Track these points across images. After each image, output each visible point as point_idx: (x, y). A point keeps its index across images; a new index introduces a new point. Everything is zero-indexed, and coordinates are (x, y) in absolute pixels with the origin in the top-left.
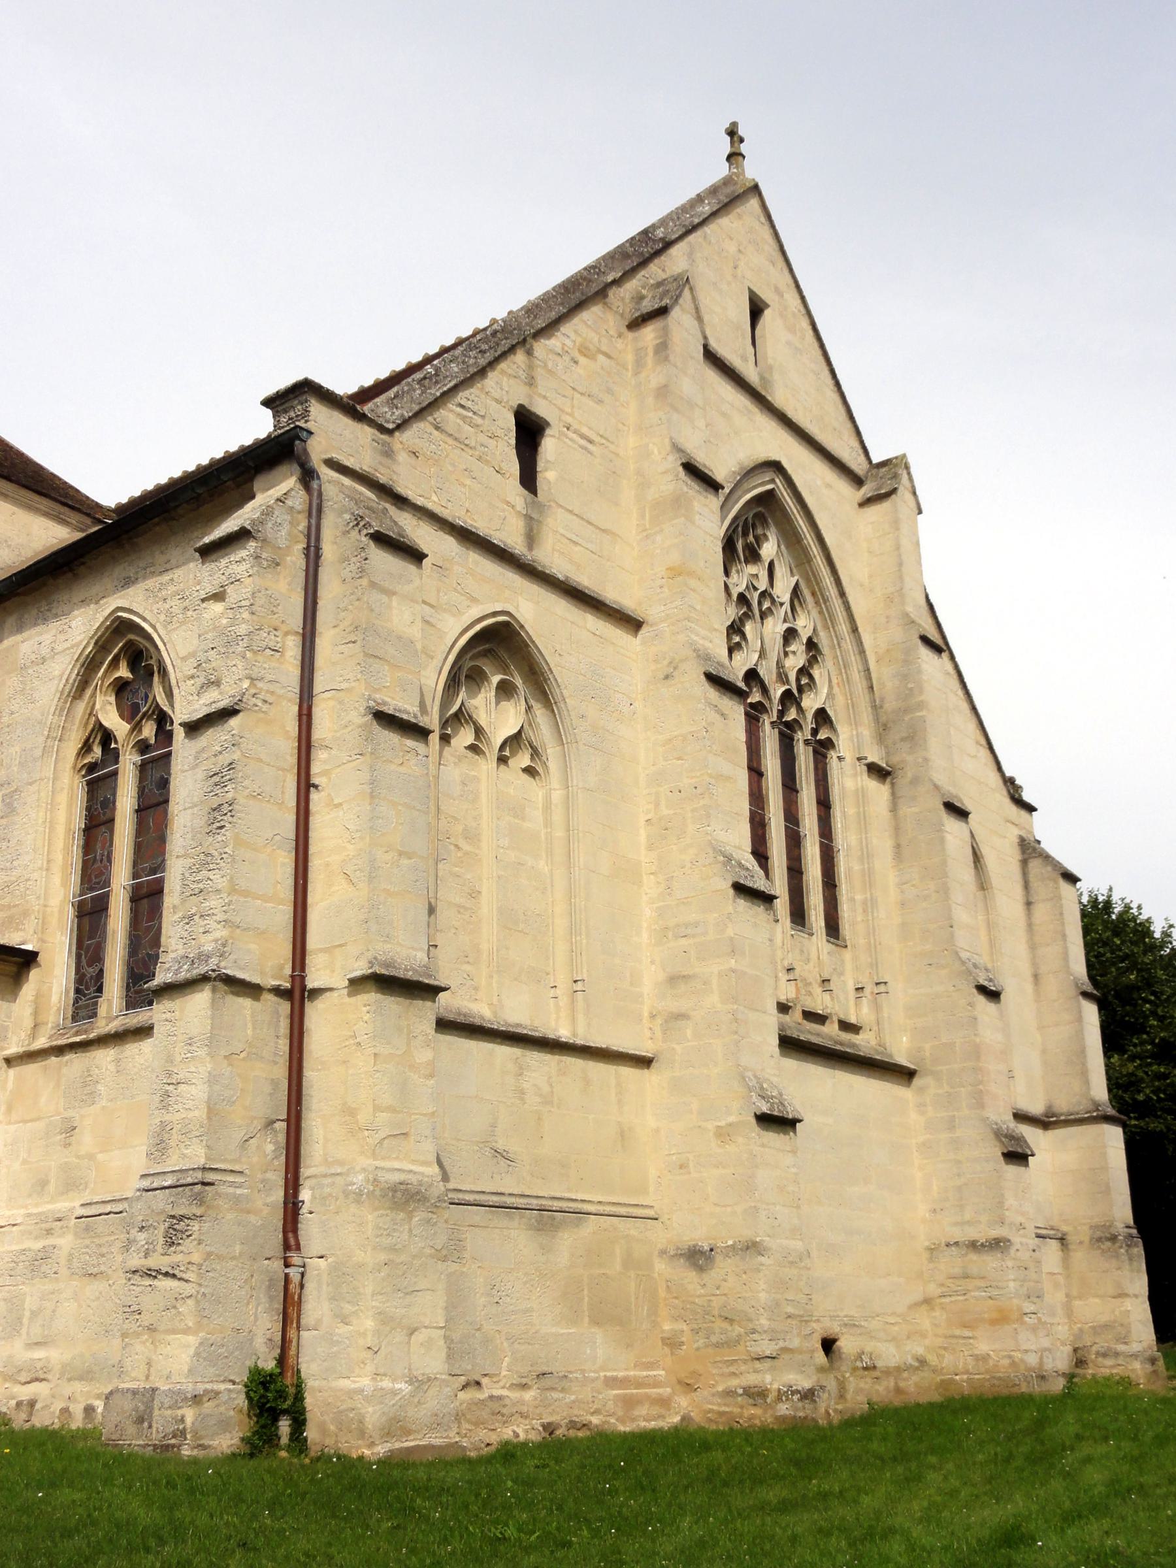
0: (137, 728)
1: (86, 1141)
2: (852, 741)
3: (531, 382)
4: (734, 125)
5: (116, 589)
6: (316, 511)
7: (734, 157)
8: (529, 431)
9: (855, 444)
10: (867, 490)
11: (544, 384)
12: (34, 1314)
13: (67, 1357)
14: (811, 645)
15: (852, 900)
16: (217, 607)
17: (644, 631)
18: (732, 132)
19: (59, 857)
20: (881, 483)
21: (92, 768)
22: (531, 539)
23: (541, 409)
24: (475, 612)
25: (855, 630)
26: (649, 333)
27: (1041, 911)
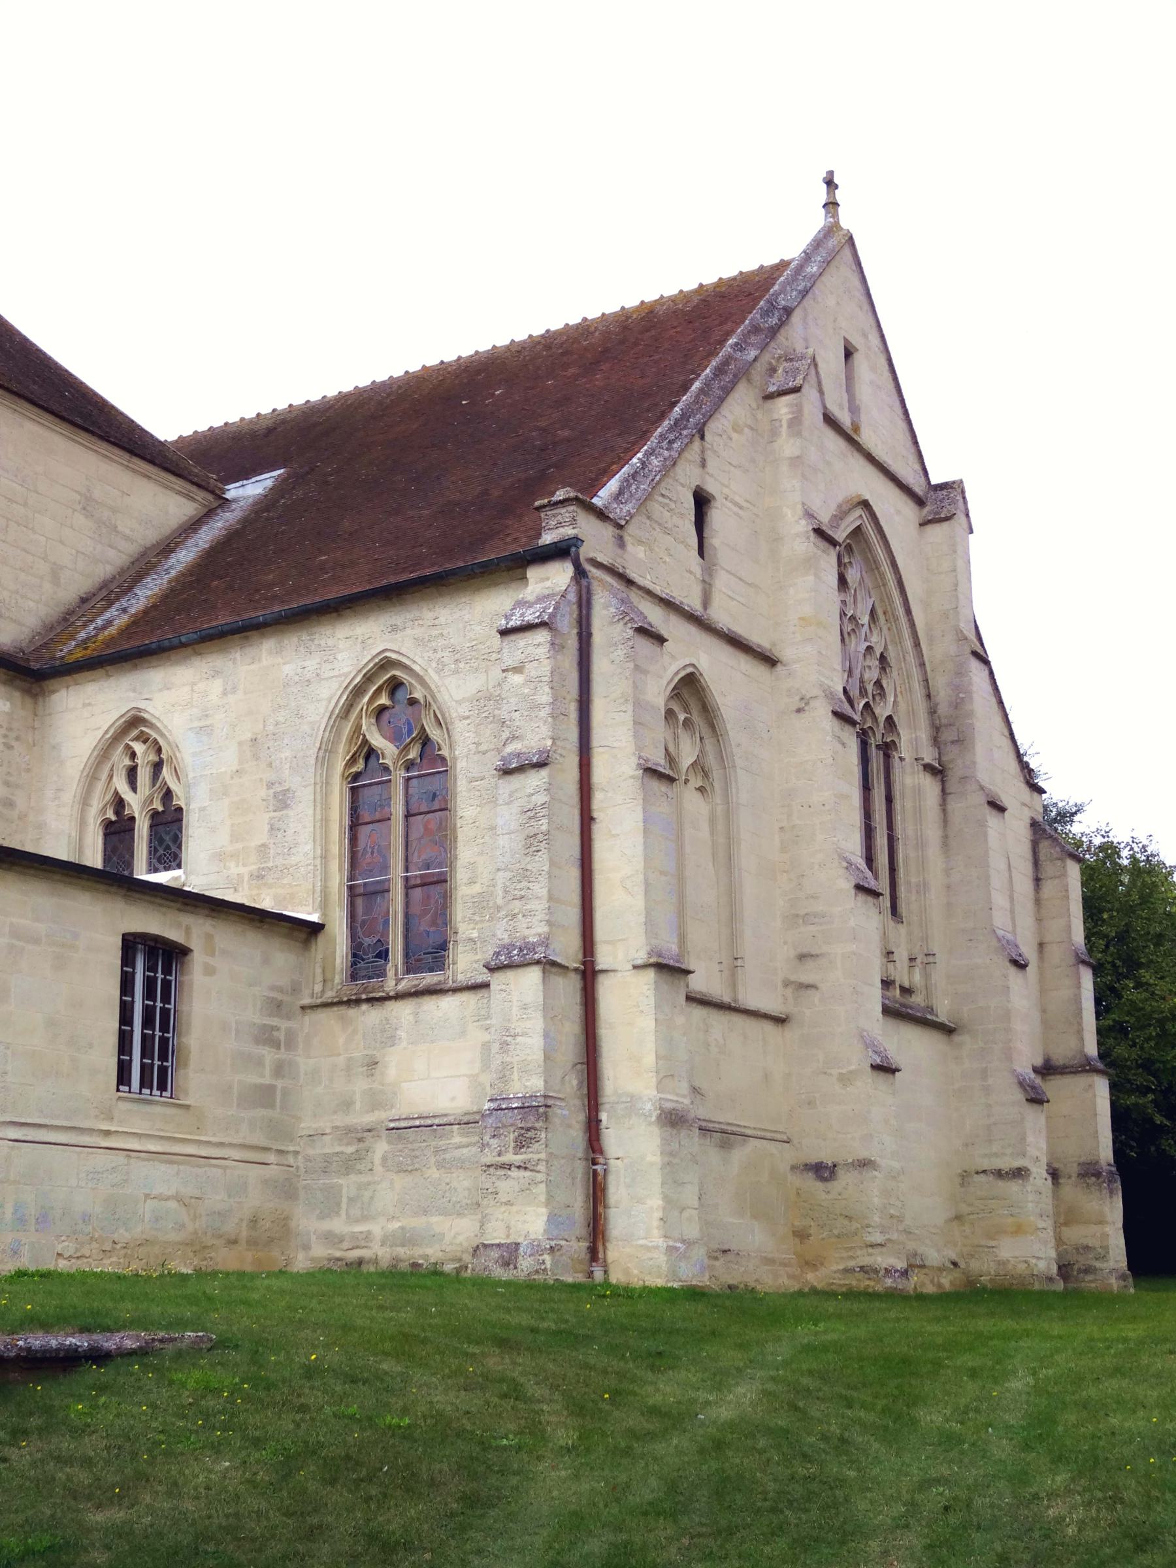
0: (406, 749)
3: (703, 464)
4: (831, 173)
6: (584, 605)
7: (831, 205)
9: (917, 467)
12: (351, 1200)
14: (883, 658)
15: (908, 883)
16: (517, 679)
17: (779, 667)
18: (830, 183)
20: (940, 504)
21: (356, 777)
22: (706, 603)
23: (711, 487)
24: (674, 668)
27: (1048, 889)
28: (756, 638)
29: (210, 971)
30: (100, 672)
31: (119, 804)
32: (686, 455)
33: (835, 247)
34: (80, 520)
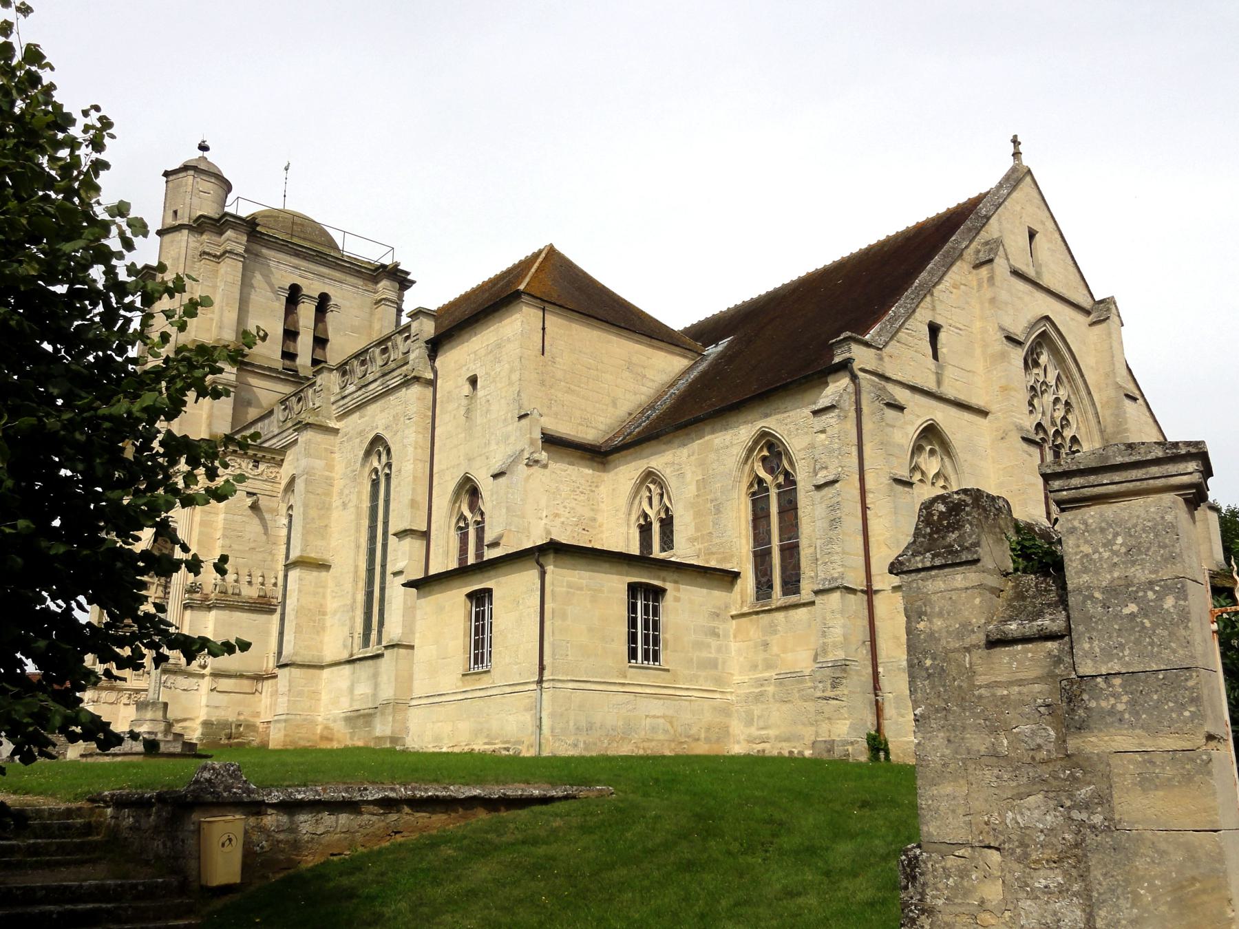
0: (776, 478)
1: (775, 649)
3: (934, 309)
4: (1015, 136)
5: (761, 418)
6: (858, 392)
7: (1017, 154)
8: (934, 330)
9: (1086, 292)
10: (1092, 318)
12: (759, 717)
13: (777, 733)
14: (1067, 404)
16: (823, 436)
17: (989, 416)
18: (1015, 141)
19: (744, 532)
20: (1101, 312)
21: (754, 494)
22: (939, 383)
23: (939, 321)
24: (920, 422)
25: (1089, 393)
26: (984, 271)
29: (677, 599)
30: (631, 450)
31: (646, 516)
33: (1018, 177)
34: (626, 374)
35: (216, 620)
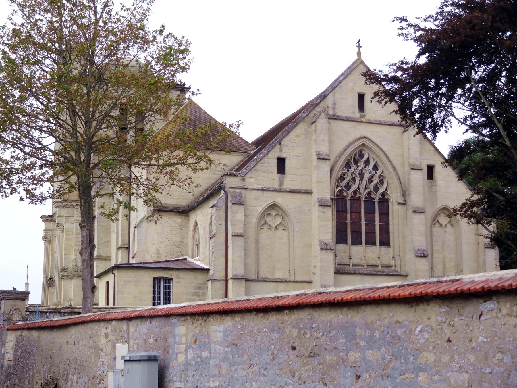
2: (394, 196)
3: (281, 150)
7: (359, 53)
11: (284, 150)
23: (283, 155)
24: (266, 204)
25: (395, 169)
28: (304, 188)
29: (178, 282)
32: (273, 150)
35: (74, 284)
